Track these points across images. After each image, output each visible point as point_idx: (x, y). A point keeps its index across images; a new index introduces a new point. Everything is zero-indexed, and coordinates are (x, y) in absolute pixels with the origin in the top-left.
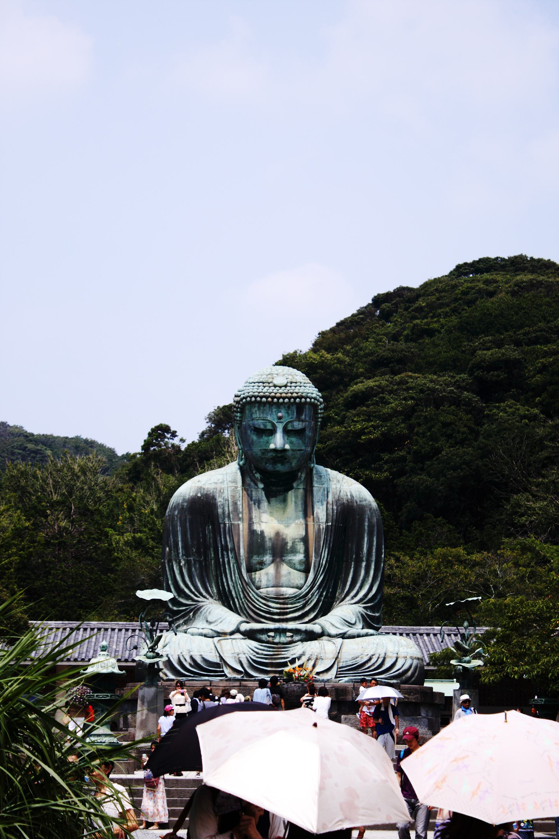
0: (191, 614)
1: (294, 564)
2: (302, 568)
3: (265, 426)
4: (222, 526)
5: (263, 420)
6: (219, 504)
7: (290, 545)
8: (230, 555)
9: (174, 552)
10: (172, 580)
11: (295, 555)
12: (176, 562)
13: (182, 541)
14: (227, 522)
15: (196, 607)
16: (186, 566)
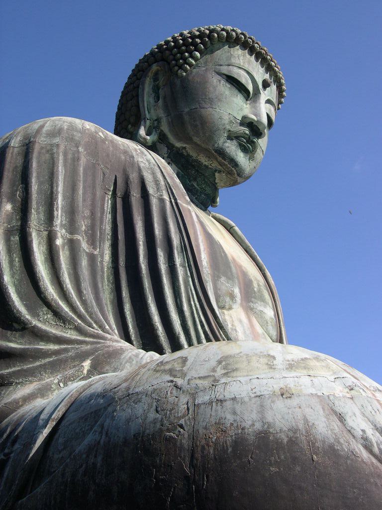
0: (87, 364)
1: (267, 323)
2: (274, 333)
3: (247, 81)
4: (154, 202)
5: (248, 73)
6: (142, 165)
7: (255, 285)
8: (178, 260)
9: (38, 213)
10: (13, 276)
11: (265, 307)
12: (39, 235)
13: (64, 197)
14: (166, 197)
15: (96, 350)
16: (67, 253)
